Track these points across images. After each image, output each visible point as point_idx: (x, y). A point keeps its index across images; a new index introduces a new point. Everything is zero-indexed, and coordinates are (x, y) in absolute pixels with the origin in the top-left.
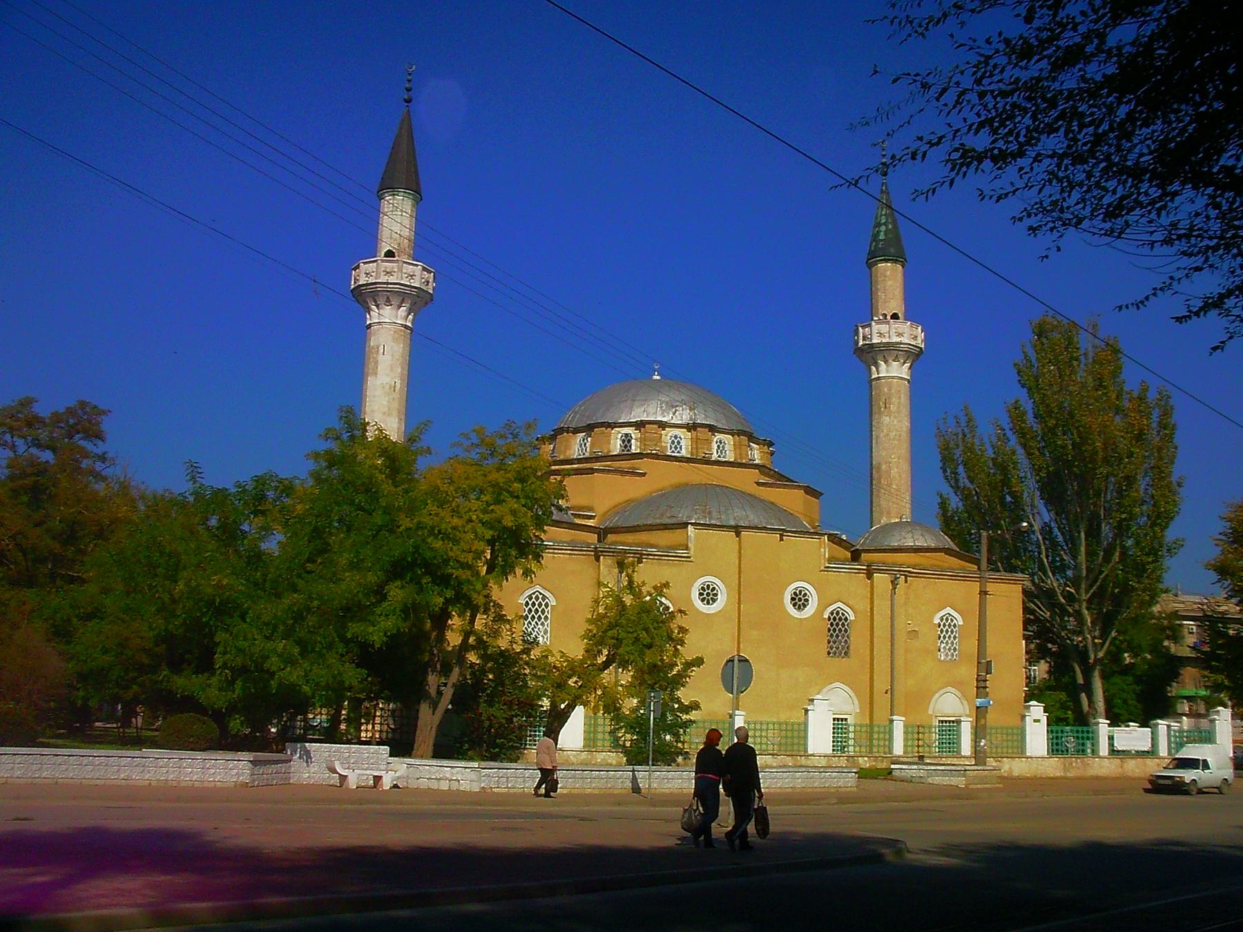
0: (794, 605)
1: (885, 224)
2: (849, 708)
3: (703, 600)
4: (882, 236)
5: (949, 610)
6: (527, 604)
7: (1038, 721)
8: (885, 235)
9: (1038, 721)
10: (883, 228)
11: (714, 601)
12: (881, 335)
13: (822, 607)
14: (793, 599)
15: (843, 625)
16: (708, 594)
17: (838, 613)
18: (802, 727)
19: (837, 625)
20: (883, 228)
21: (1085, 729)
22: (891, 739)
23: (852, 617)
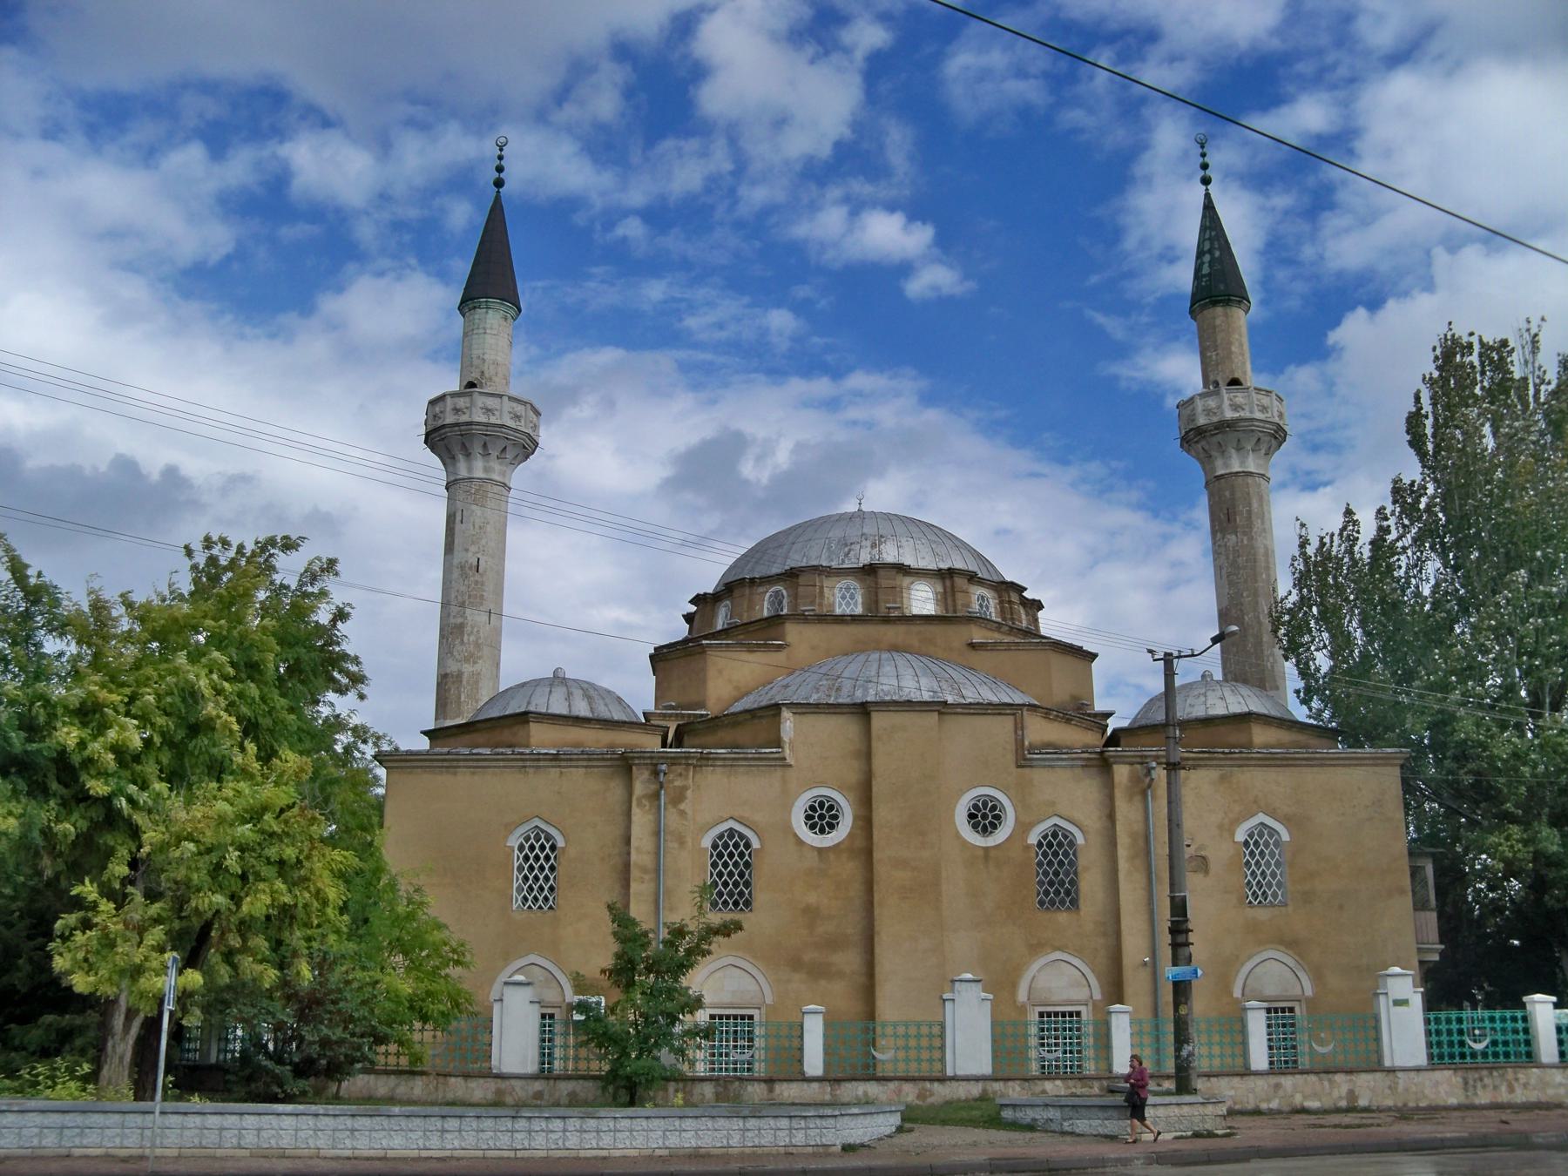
0: (975, 826)
1: (1210, 251)
2: (1081, 994)
3: (812, 827)
4: (1206, 270)
5: (1261, 818)
6: (521, 848)
7: (1404, 1002)
8: (1210, 266)
9: (1404, 1002)
10: (1207, 258)
11: (832, 827)
12: (1208, 412)
13: (1023, 828)
14: (971, 816)
15: (1066, 854)
16: (822, 817)
17: (1055, 835)
18: (936, 1030)
19: (1056, 854)
20: (1207, 258)
21: (1519, 1014)
22: (1244, 1044)
23: (1080, 840)
